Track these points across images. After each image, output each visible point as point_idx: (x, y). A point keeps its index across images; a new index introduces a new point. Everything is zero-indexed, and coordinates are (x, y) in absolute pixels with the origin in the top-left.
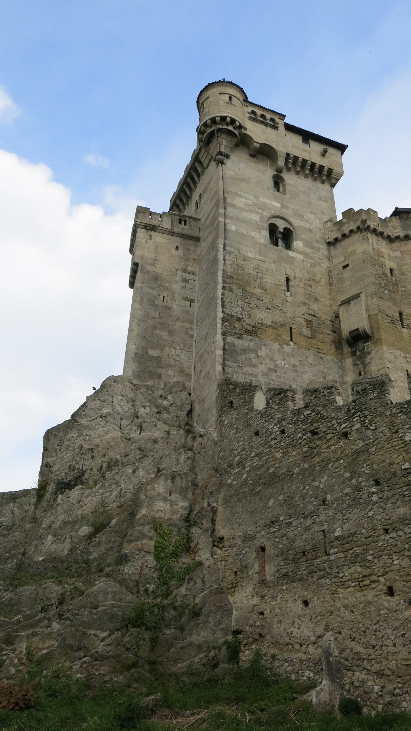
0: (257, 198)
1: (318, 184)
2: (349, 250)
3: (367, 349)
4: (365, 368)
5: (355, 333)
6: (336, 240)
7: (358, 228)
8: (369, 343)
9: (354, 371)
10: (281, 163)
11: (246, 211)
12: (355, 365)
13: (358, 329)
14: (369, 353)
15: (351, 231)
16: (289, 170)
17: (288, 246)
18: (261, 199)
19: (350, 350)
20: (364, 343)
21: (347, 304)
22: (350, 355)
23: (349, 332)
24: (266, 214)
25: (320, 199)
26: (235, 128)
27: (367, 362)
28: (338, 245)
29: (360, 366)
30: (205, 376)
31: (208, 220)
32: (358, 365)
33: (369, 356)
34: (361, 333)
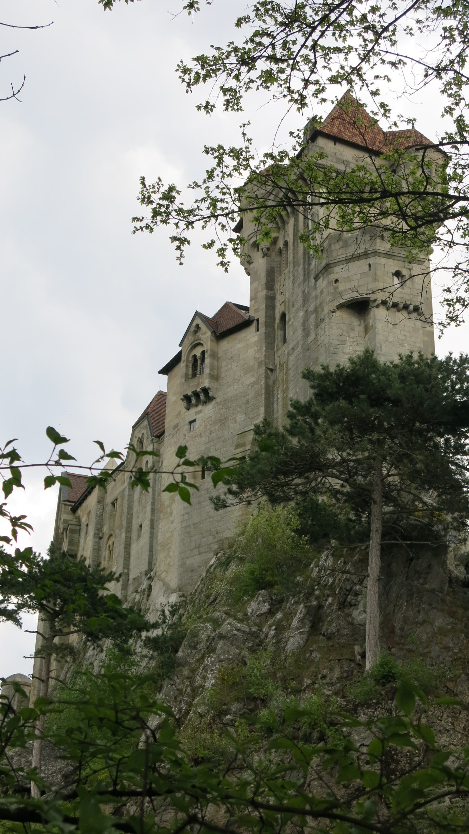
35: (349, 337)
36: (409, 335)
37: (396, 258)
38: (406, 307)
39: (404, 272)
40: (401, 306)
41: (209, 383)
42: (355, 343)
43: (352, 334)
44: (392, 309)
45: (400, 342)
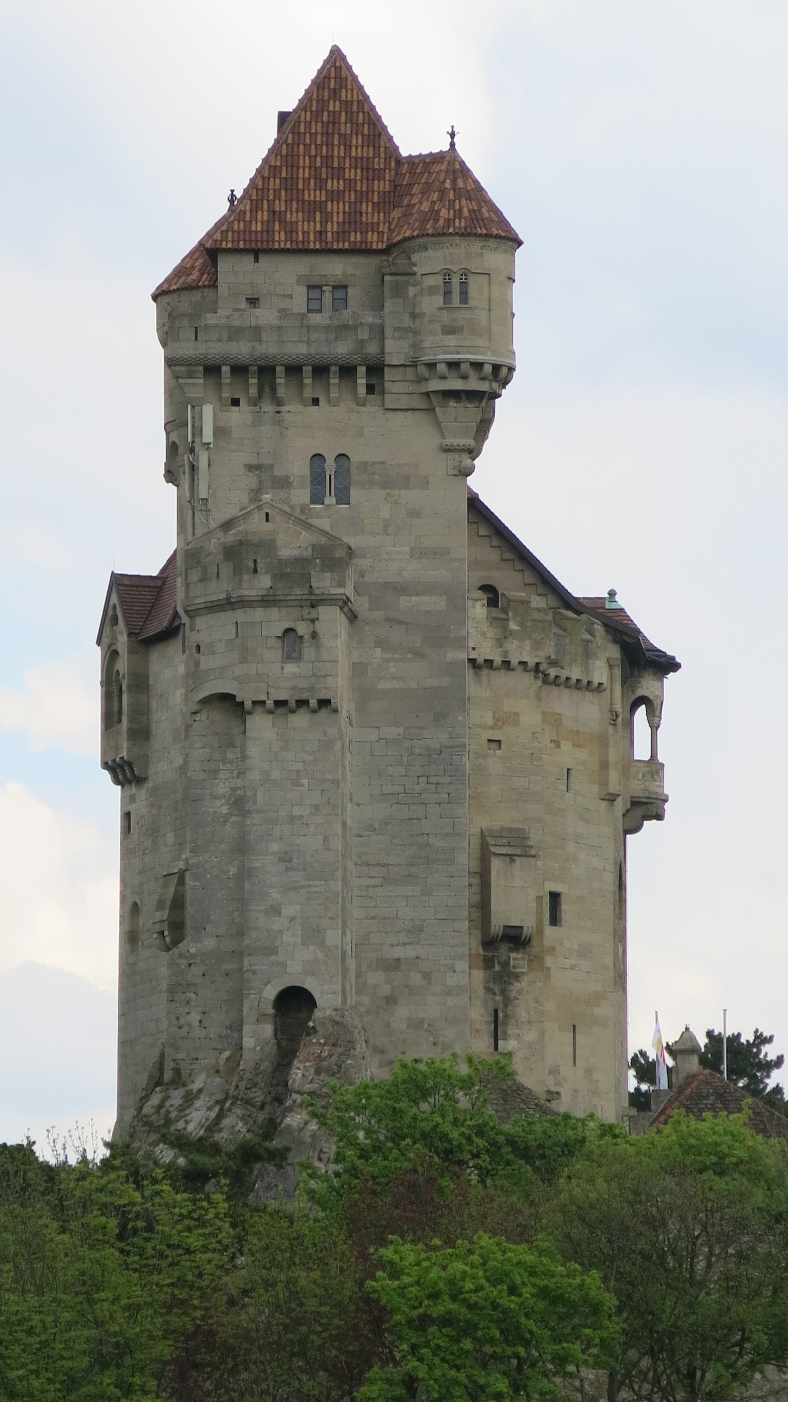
2: (508, 706)
3: (514, 967)
4: (506, 1006)
5: (512, 932)
6: (489, 663)
7: (537, 664)
8: (520, 956)
9: (485, 1003)
12: (488, 990)
13: (521, 927)
14: (517, 977)
15: (523, 663)
19: (482, 953)
20: (511, 950)
21: (508, 859)
22: (481, 964)
23: (504, 926)
27: (513, 994)
28: (485, 672)
29: (498, 998)
30: (416, 1024)
31: (405, 602)
32: (494, 994)
33: (517, 985)
34: (523, 938)
35: (224, 761)
36: (311, 758)
37: (285, 604)
38: (302, 703)
39: (302, 629)
40: (292, 704)
41: (129, 749)
42: (235, 774)
43: (230, 755)
44: (280, 711)
45: (294, 777)
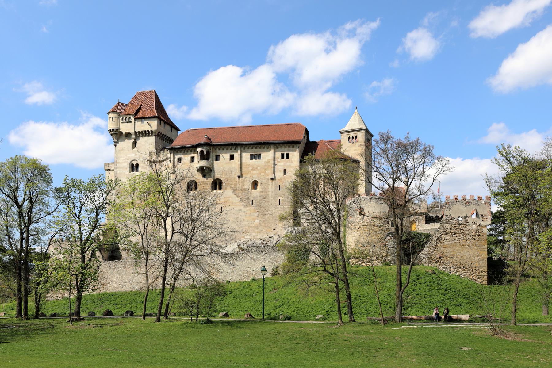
0: (126, 155)
1: (151, 138)
10: (134, 137)
11: (122, 163)
16: (139, 136)
17: (137, 170)
18: (128, 155)
24: (129, 161)
25: (149, 144)
26: (115, 132)
